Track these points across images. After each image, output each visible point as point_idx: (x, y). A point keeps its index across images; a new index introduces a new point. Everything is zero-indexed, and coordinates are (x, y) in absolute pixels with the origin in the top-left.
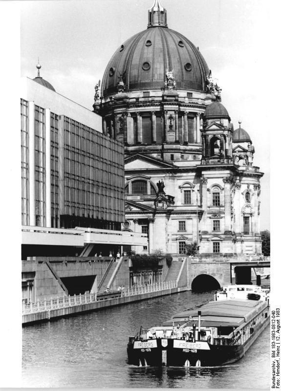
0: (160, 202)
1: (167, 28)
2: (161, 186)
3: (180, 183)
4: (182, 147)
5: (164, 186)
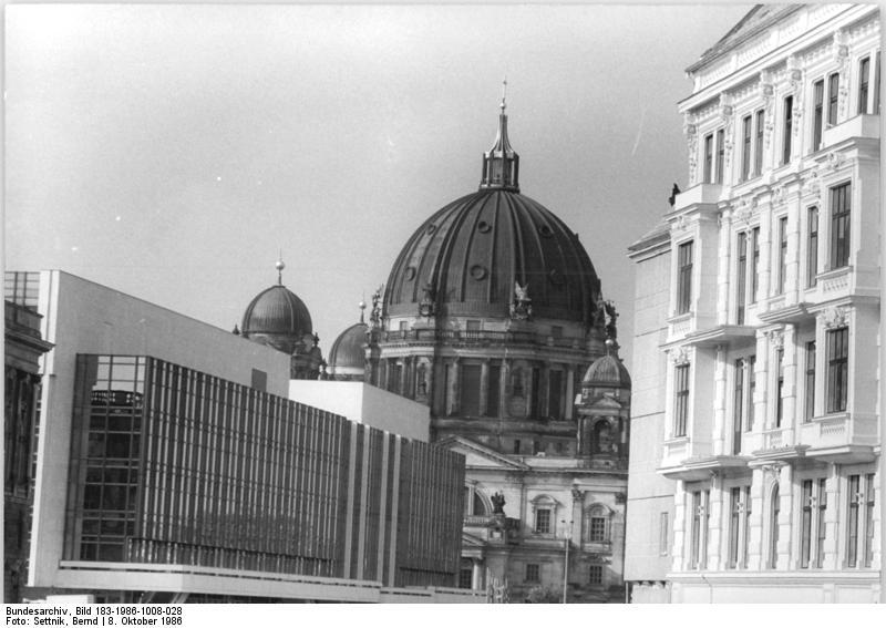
0: (498, 529)
1: (518, 192)
2: (499, 502)
3: (532, 495)
4: (538, 426)
5: (503, 503)
